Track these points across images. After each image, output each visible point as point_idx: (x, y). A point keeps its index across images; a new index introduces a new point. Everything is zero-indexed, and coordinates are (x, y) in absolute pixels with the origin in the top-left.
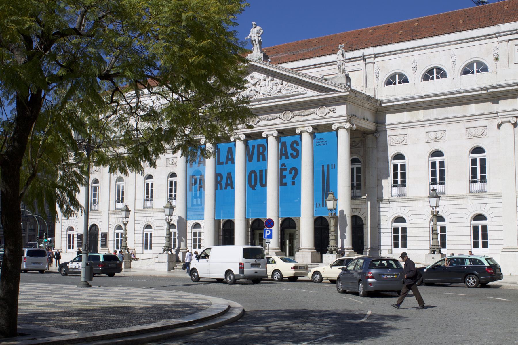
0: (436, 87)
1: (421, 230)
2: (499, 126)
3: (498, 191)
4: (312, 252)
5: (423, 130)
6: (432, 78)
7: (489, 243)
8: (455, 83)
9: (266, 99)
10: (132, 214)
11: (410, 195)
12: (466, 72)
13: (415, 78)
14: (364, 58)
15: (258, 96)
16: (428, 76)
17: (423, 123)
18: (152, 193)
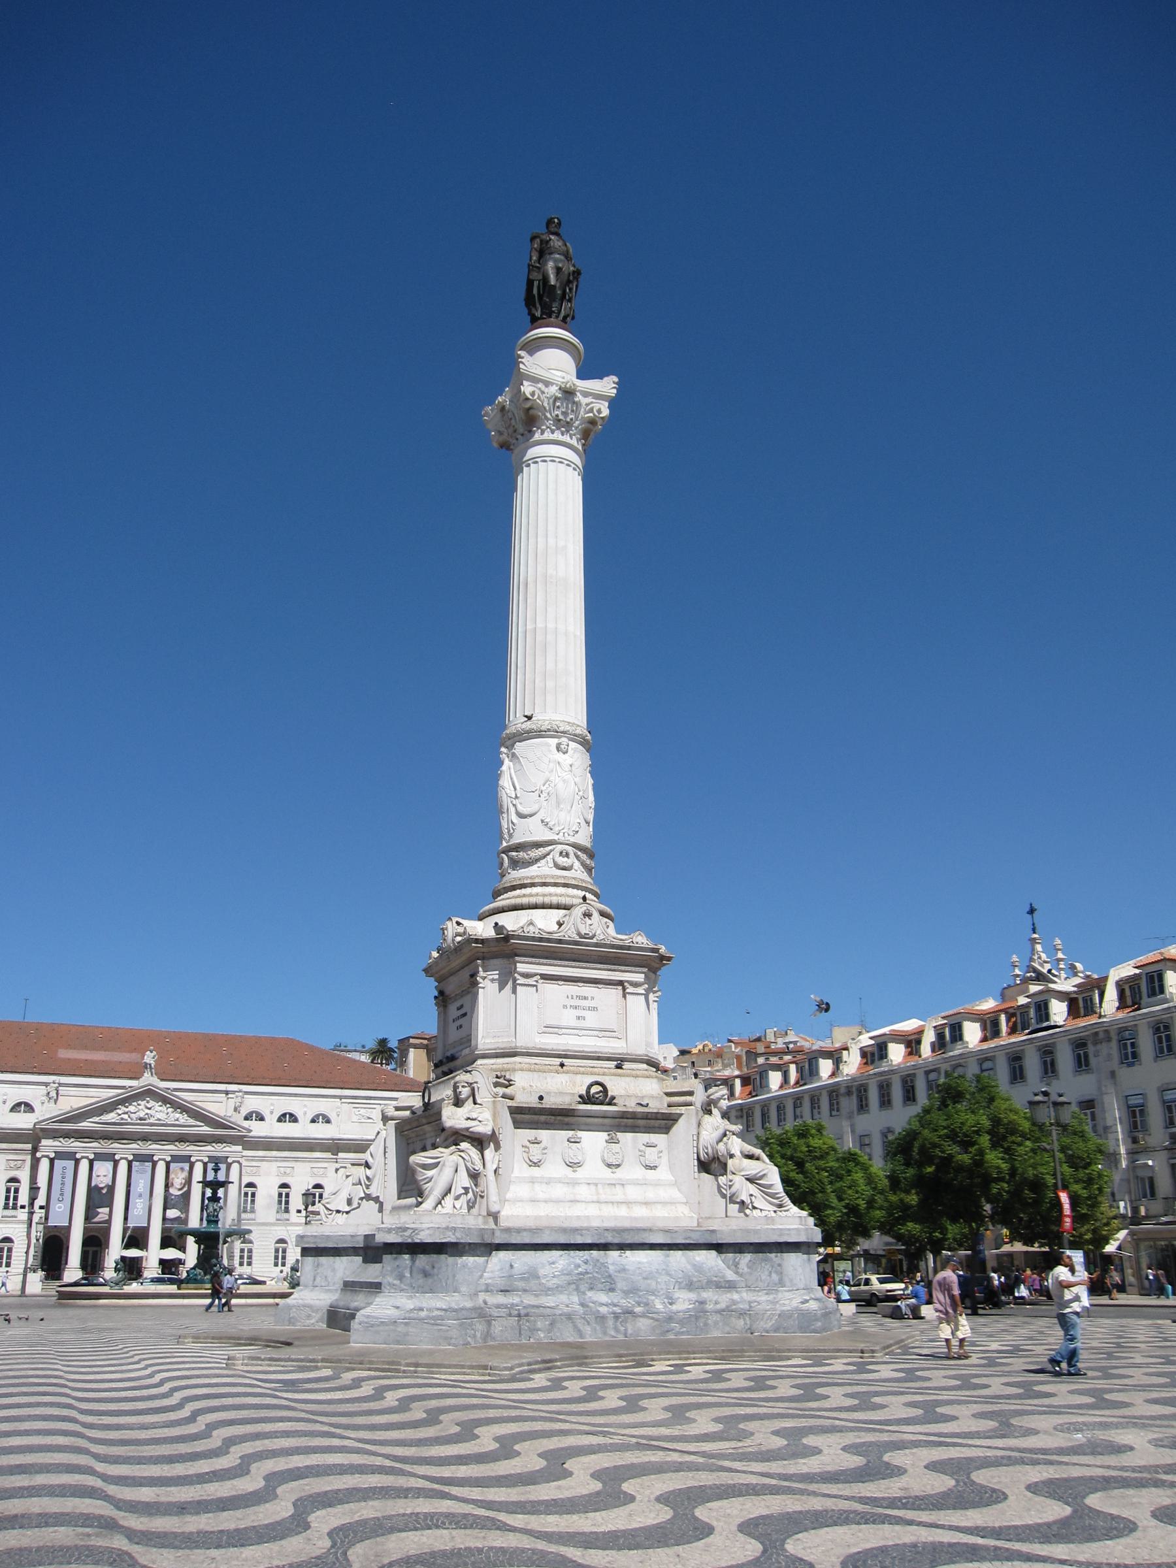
0: (288, 1130)
2: (337, 1170)
5: (275, 1165)
8: (302, 1130)
11: (258, 1221)
12: (313, 1121)
13: (272, 1119)
14: (227, 1093)
15: (152, 1121)
17: (276, 1159)
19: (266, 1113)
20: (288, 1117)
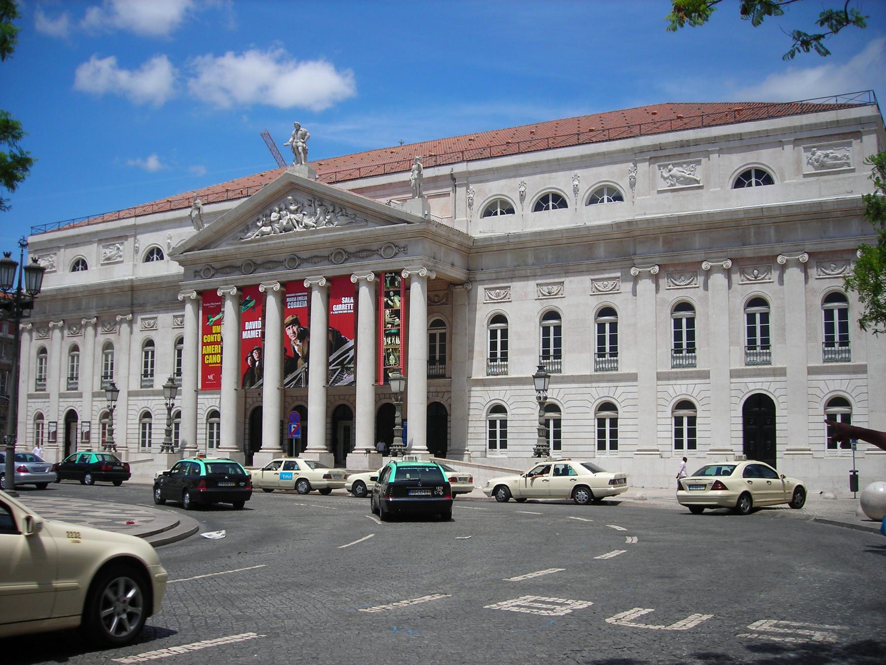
0: (553, 221)
1: (527, 423)
3: (633, 371)
4: (274, 453)
6: (547, 208)
7: (619, 443)
9: (314, 233)
10: (122, 395)
11: (512, 375)
12: (593, 200)
14: (452, 177)
15: (299, 229)
16: (541, 205)
18: (152, 366)
19: (514, 200)
20: (551, 201)
